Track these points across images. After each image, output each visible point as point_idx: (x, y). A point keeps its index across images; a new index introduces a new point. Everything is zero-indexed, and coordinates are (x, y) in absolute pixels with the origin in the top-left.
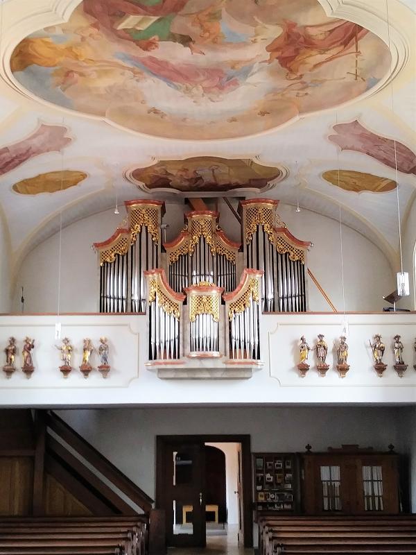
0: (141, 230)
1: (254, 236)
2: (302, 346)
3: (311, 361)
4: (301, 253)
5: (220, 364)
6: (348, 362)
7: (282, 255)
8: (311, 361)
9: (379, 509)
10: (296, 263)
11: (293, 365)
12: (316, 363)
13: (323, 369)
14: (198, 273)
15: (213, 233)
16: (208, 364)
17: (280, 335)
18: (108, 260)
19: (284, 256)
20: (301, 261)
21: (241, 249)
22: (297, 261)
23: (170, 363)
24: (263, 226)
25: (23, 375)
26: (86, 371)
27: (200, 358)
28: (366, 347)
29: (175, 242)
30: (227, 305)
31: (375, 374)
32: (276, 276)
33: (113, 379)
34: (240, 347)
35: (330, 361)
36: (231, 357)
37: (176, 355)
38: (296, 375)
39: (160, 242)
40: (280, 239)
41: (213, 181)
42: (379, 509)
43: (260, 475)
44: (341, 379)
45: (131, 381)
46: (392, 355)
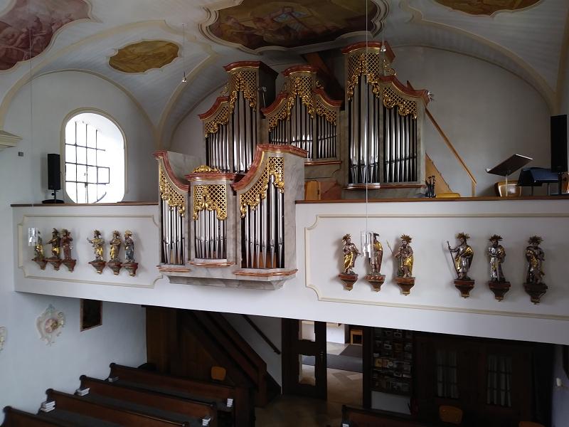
1: (356, 89)
2: (346, 248)
4: (413, 105)
5: (229, 275)
6: (415, 273)
7: (390, 110)
8: (360, 269)
9: (506, 405)
10: (407, 118)
11: (337, 272)
12: (368, 271)
13: (376, 283)
16: (216, 274)
17: (316, 231)
20: (413, 116)
22: (409, 115)
24: (366, 76)
26: (117, 267)
27: (207, 266)
28: (445, 251)
30: (239, 197)
31: (457, 293)
32: (381, 136)
33: (141, 278)
35: (387, 270)
36: (244, 266)
37: (180, 260)
38: (339, 287)
39: (258, 108)
40: (388, 90)
41: (325, 29)
42: (506, 405)
43: (378, 341)
44: (404, 295)
46: (486, 265)
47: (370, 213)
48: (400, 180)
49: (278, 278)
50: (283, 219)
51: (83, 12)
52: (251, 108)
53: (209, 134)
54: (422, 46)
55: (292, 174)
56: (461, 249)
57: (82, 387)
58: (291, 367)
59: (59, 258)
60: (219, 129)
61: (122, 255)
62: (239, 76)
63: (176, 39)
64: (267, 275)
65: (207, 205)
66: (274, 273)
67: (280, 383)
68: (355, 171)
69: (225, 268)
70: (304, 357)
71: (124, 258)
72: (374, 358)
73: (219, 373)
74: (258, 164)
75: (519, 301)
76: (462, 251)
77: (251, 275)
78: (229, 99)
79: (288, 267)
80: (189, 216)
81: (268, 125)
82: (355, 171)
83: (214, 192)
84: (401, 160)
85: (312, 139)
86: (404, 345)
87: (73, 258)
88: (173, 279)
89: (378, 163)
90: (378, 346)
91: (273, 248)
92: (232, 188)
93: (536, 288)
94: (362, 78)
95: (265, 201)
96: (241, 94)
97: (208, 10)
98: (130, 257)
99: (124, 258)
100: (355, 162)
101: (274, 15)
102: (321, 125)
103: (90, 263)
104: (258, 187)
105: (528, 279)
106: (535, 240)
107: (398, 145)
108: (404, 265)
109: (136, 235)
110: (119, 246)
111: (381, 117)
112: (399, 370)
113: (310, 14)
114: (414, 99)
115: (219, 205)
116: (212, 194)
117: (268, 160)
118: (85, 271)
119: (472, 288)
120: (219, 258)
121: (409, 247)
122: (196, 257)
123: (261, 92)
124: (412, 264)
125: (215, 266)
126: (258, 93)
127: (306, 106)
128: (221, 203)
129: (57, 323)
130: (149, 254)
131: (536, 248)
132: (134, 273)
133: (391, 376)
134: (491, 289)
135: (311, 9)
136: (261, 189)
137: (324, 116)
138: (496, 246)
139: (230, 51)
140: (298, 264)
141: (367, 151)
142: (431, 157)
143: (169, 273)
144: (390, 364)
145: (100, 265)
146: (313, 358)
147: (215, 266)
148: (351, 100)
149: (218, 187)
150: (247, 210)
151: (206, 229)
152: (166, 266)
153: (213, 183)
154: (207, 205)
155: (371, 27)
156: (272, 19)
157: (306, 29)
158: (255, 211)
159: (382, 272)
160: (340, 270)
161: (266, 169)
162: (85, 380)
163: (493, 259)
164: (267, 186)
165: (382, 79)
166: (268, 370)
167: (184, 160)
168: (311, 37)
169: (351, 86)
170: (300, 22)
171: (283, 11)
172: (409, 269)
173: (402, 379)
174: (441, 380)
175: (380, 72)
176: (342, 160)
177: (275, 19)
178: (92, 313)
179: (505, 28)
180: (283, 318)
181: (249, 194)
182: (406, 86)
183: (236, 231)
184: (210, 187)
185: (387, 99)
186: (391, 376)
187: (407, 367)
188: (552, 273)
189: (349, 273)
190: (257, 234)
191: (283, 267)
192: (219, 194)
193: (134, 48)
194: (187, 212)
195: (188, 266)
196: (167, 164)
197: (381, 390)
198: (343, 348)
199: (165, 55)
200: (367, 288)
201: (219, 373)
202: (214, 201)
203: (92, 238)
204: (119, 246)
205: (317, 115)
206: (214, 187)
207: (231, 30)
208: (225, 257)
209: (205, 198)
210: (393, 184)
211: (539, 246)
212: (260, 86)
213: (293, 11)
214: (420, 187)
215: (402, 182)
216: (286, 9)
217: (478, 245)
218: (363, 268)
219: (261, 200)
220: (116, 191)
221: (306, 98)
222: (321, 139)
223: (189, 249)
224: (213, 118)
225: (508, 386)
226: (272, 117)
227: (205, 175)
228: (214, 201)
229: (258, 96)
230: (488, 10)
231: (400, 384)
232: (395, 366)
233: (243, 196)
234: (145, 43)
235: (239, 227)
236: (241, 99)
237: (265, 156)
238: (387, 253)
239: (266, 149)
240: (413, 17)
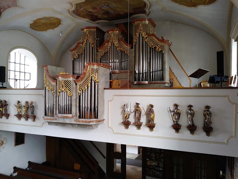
3: (132, 119)
4: (162, 47)
5: (73, 122)
6: (155, 121)
7: (153, 49)
8: (132, 119)
10: (160, 52)
11: (122, 121)
12: (135, 121)
13: (138, 125)
14: (113, 61)
15: (119, 40)
16: (67, 121)
18: (75, 57)
19: (154, 49)
20: (163, 52)
21: (132, 48)
22: (161, 51)
26: (27, 118)
27: (64, 117)
28: (168, 112)
29: (101, 46)
30: (78, 86)
31: (173, 131)
32: (149, 60)
35: (143, 120)
36: (80, 117)
37: (52, 115)
38: (123, 127)
39: (95, 47)
40: (152, 40)
44: (151, 132)
45: (43, 124)
46: (186, 118)
47: (129, 94)
48: (157, 80)
49: (95, 123)
50: (98, 96)
51: (14, 3)
52: (92, 47)
53: (74, 58)
54: (169, 21)
55: (102, 76)
56: (175, 111)
57: (14, 172)
58: (110, 165)
59: (2, 113)
60: (78, 57)
61: (28, 112)
62: (87, 33)
63: (59, 16)
64: (90, 122)
65: (63, 90)
66: (93, 121)
67: (105, 172)
68: (137, 76)
69: (71, 118)
70: (117, 160)
71: (30, 113)
72: (147, 161)
73: (77, 167)
74: (86, 71)
75: (201, 135)
76: (176, 113)
77: (83, 122)
78: (83, 43)
79: (100, 118)
80: (56, 94)
82: (137, 76)
83: (68, 85)
85: (118, 61)
86: (160, 155)
87: (8, 113)
88: (50, 123)
89: (147, 72)
90: (149, 155)
91: (93, 110)
92: (75, 82)
93: (208, 130)
94: (140, 34)
95: (89, 88)
96: (88, 41)
97: (71, 4)
98: (32, 113)
99: (30, 113)
100: (137, 72)
101: (100, 6)
102: (123, 54)
103: (15, 115)
104: (86, 82)
105: (204, 125)
106: (208, 107)
107: (156, 65)
108: (150, 118)
109: (35, 103)
110: (28, 108)
111: (149, 52)
112: (158, 166)
113: (117, 6)
114: (163, 44)
115: (69, 90)
116: (66, 85)
117: (91, 69)
118: (13, 119)
119: (180, 129)
120: (69, 114)
121: (152, 109)
122: (59, 113)
123: (97, 41)
124: (154, 117)
125: (67, 117)
126: (95, 40)
127: (116, 47)
128: (70, 89)
129: (3, 142)
130: (40, 112)
131: (208, 111)
132: (34, 120)
133: (154, 169)
134: (188, 129)
135: (117, 4)
136: (87, 83)
137: (124, 51)
138: (190, 110)
139: (84, 22)
140: (105, 117)
141: (142, 67)
142: (173, 71)
143: (47, 120)
144: (154, 164)
145: (19, 116)
146: (120, 160)
147: (67, 117)
148: (136, 44)
149: (69, 82)
150: (81, 92)
151: (63, 102)
152: (46, 117)
153: (66, 79)
154: (63, 90)
155: (144, 12)
156: (100, 8)
157: (117, 13)
159: (141, 121)
160: (123, 120)
161: (90, 73)
162: (16, 169)
163: (189, 115)
164: (90, 81)
165: (149, 35)
166: (99, 164)
167: (56, 69)
168: (119, 16)
169: (135, 38)
170: (113, 10)
171: (105, 5)
172: (153, 120)
173: (159, 171)
174: (175, 171)
175: (148, 32)
176: (132, 71)
177: (101, 8)
178: (20, 138)
179: (203, 13)
180: (107, 143)
181: (82, 85)
182: (161, 39)
183: (76, 101)
184: (65, 82)
185: (151, 44)
186: (154, 169)
187: (161, 165)
188: (215, 123)
189: (126, 121)
190: (86, 104)
191: (97, 118)
192: (69, 84)
193: (41, 20)
194: (55, 93)
195: (55, 117)
196: (47, 71)
197: (149, 175)
198: (137, 156)
199: (55, 24)
200: (135, 128)
201: (77, 167)
202: (67, 88)
203: (16, 104)
204: (28, 108)
205: (121, 51)
206: (67, 81)
207: (83, 13)
208: (71, 114)
209: (62, 86)
210: (154, 82)
211: (209, 110)
212: (97, 37)
213: (109, 5)
214: (165, 83)
215: (155, 81)
216: (106, 4)
217: (183, 109)
218: (132, 119)
219: (88, 87)
220: (33, 83)
221: (116, 43)
222: (123, 62)
223: (56, 110)
224: (76, 52)
225: (205, 175)
226: (102, 52)
227: (63, 76)
228: (67, 88)
229: (95, 42)
230: (194, 5)
231: (158, 173)
232: (156, 164)
233: (80, 86)
234: (45, 18)
236: (88, 43)
237: (90, 68)
238: (143, 113)
239: (89, 64)
240: (163, 8)
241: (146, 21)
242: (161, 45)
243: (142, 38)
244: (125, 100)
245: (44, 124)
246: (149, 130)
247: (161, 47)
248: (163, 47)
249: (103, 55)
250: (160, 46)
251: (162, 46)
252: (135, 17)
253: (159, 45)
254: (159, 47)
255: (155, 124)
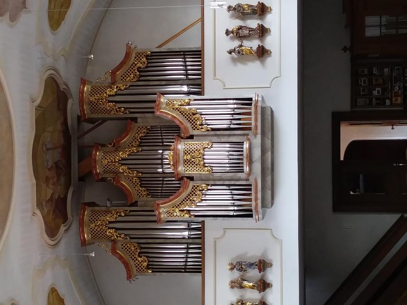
0: (113, 228)
2: (239, 55)
3: (254, 44)
4: (139, 55)
5: (257, 141)
6: (255, 4)
7: (141, 76)
8: (254, 44)
10: (149, 61)
12: (256, 39)
13: (263, 31)
14: (160, 166)
16: (257, 153)
17: (227, 79)
18: (145, 264)
20: (148, 56)
22: (147, 59)
23: (257, 195)
24: (110, 96)
25: (268, 290)
26: (264, 285)
27: (250, 162)
30: (195, 132)
32: (164, 83)
33: (273, 256)
34: (239, 119)
35: (253, 23)
36: (250, 129)
37: (248, 188)
38: (269, 60)
39: (129, 209)
40: (123, 77)
41: (60, 150)
44: (272, 11)
45: (275, 237)
53: (148, 268)
54: (86, 66)
81: (145, 198)
84: (187, 70)
111: (146, 83)
136: (189, 114)
158: (207, 120)
174: (395, 30)
184: (186, 154)
195: (252, 181)
221: (122, 155)
229: (115, 208)
233: (194, 130)
235: (218, 132)
237: (164, 108)
241: (90, 57)
242: (136, 58)
243: (117, 96)
244: (223, 56)
245: (276, 237)
246: (269, 15)
247: (139, 58)
248: (139, 54)
249: (145, 191)
250: (137, 60)
251: (137, 56)
252: (72, 119)
253: (134, 63)
254: (139, 61)
255: (259, 2)
